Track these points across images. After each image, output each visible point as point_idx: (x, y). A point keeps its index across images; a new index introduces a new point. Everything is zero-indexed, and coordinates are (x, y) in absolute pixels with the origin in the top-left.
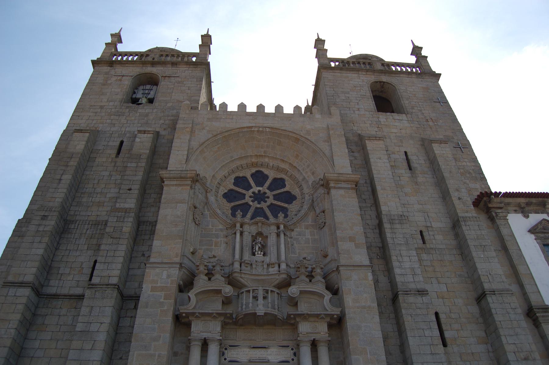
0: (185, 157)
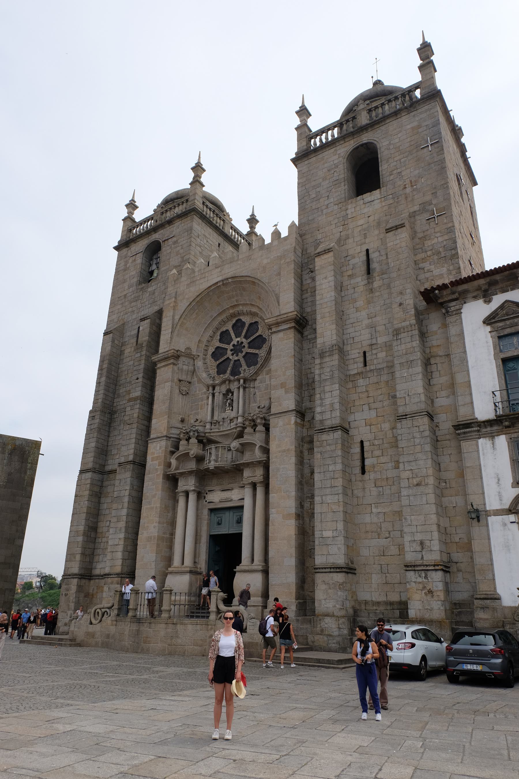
0: (170, 336)
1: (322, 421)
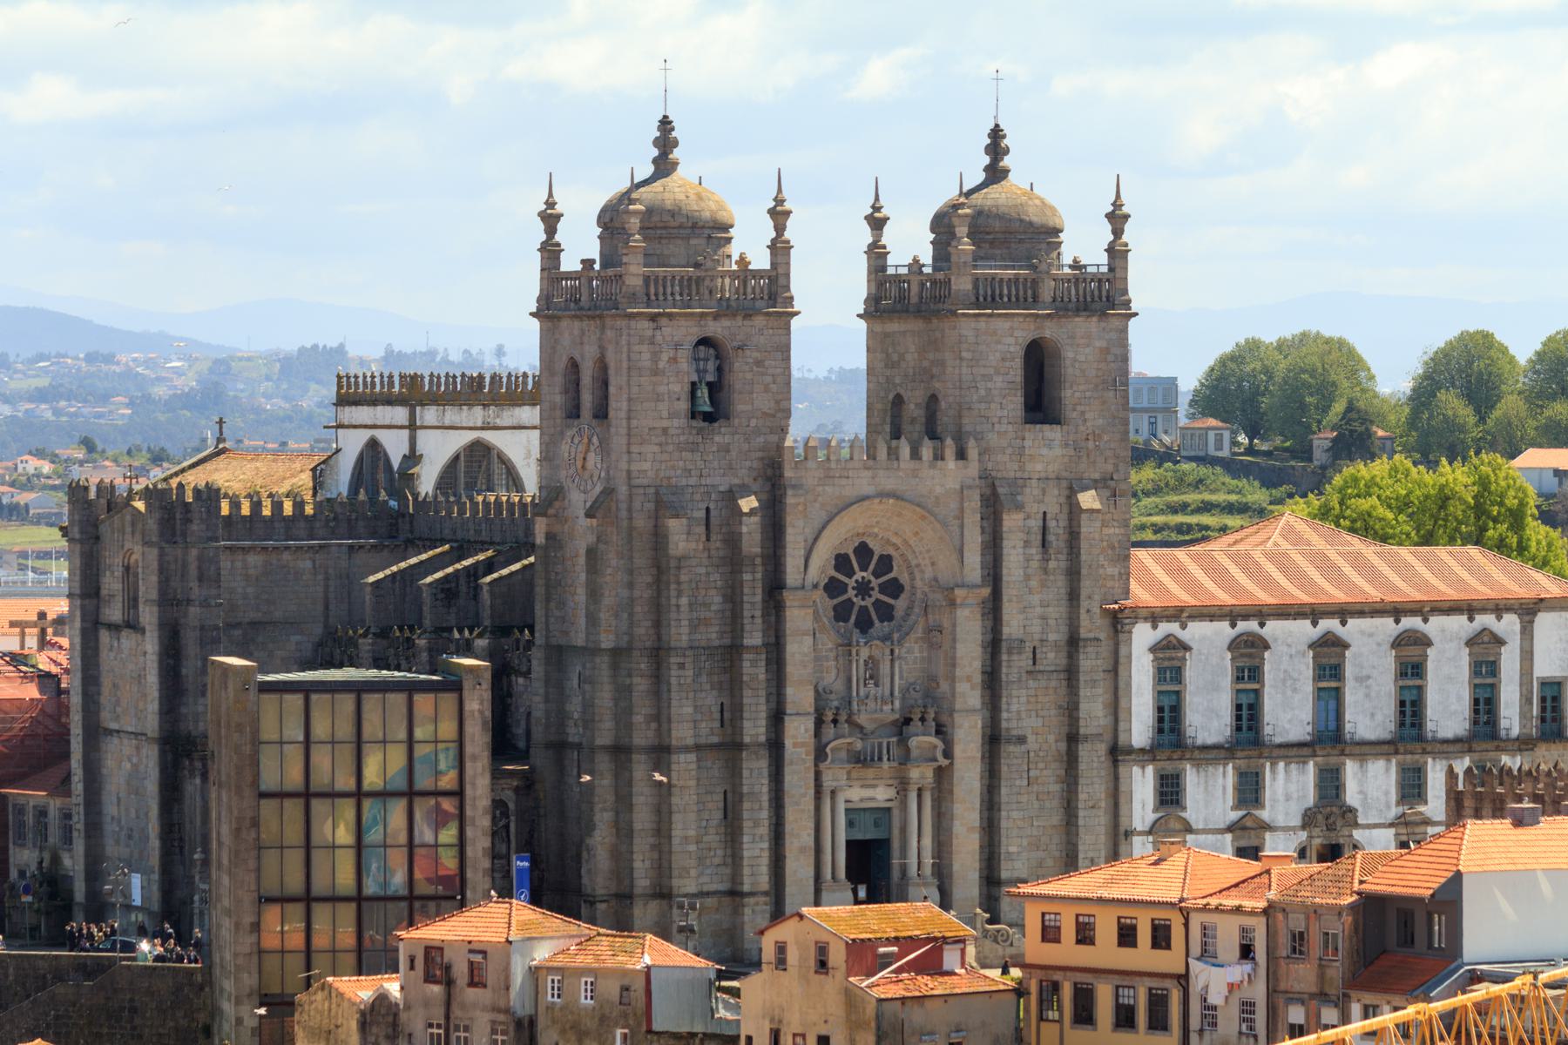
1: (1008, 729)
